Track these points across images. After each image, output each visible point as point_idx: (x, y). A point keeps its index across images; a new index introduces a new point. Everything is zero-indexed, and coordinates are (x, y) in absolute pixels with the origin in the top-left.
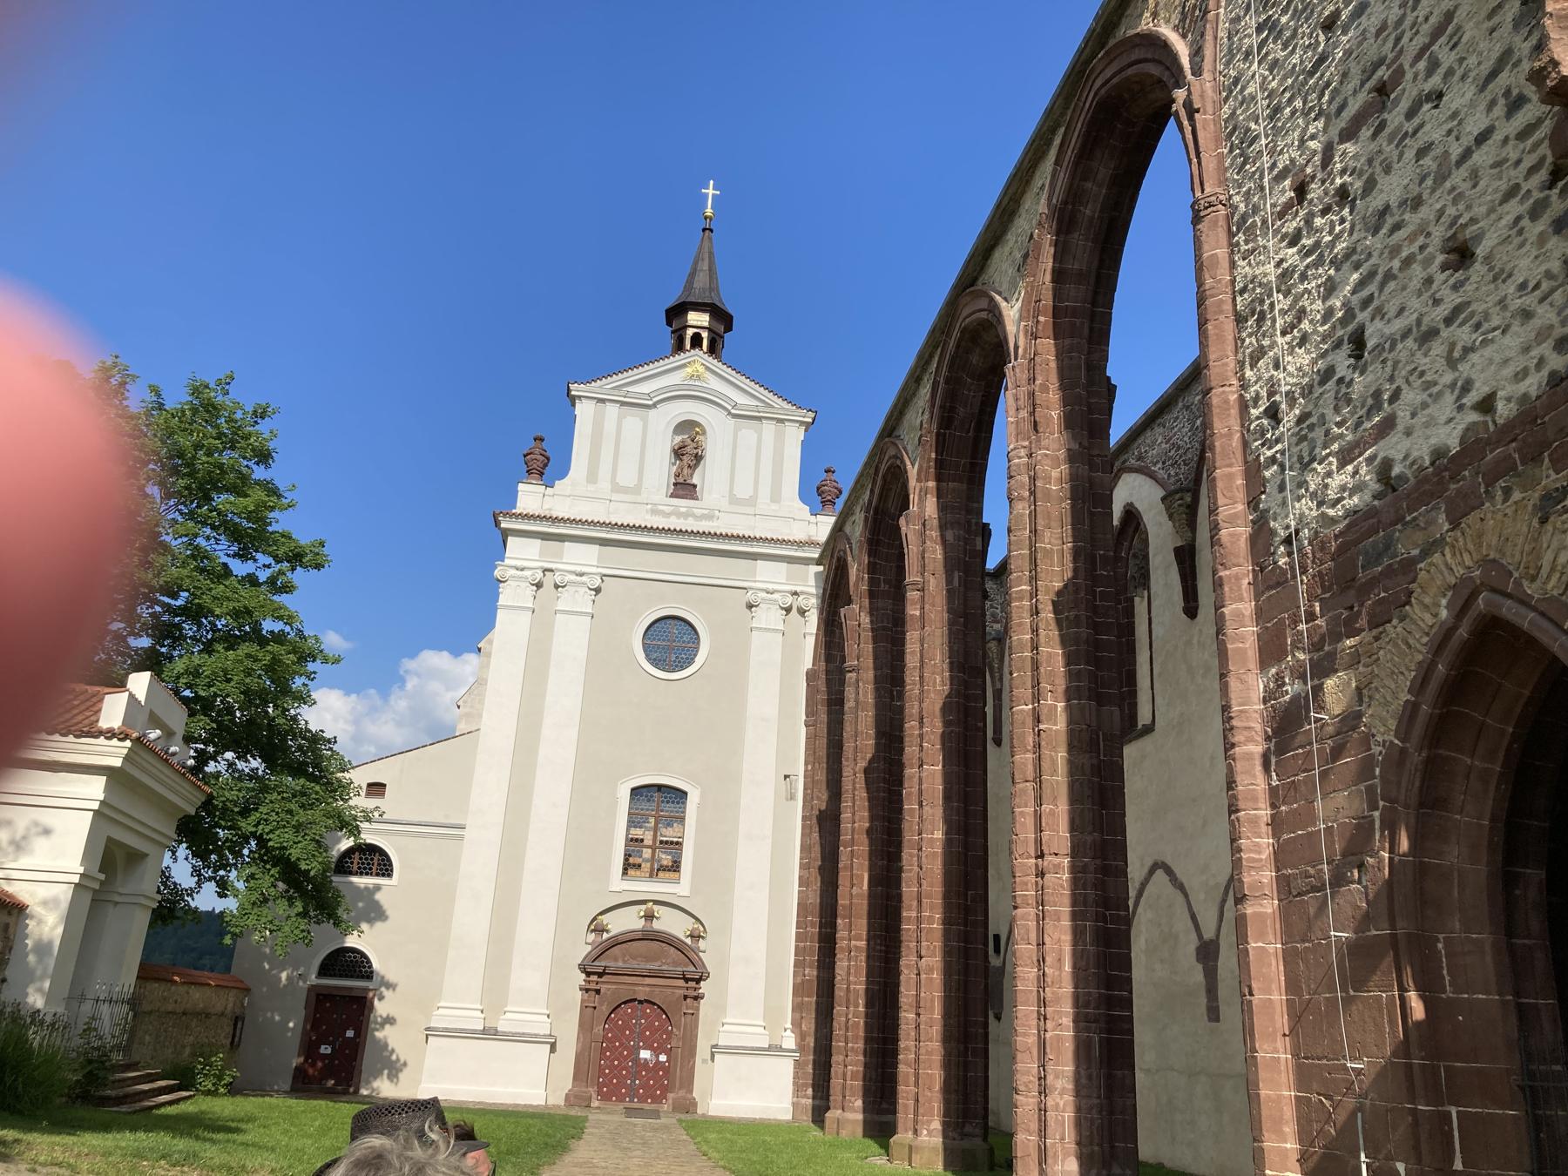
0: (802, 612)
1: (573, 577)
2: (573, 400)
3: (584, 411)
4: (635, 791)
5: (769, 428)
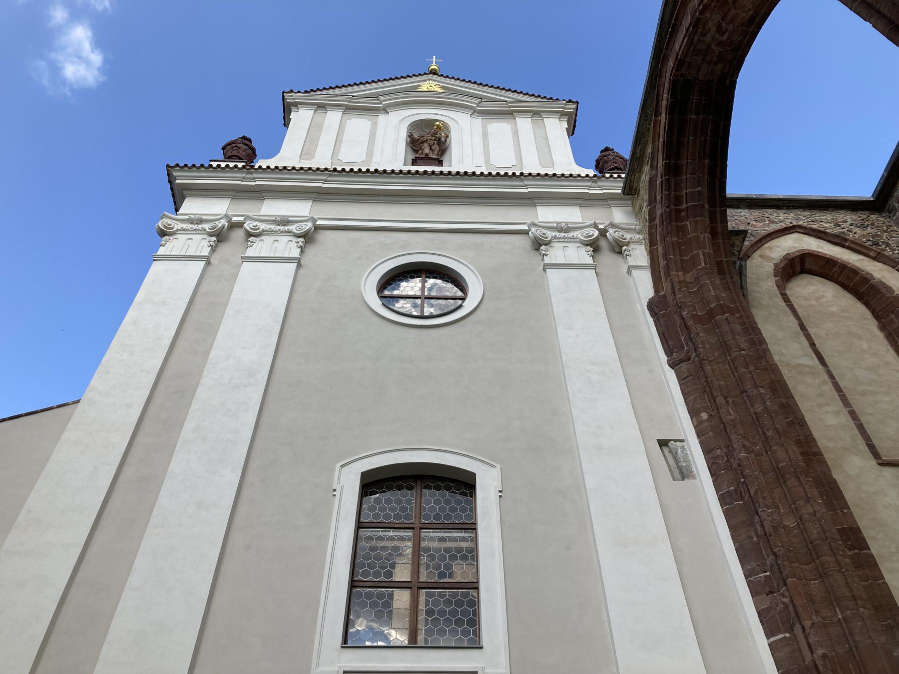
0: (618, 248)
1: (273, 227)
2: (287, 110)
3: (301, 118)
4: (373, 483)
5: (524, 124)
